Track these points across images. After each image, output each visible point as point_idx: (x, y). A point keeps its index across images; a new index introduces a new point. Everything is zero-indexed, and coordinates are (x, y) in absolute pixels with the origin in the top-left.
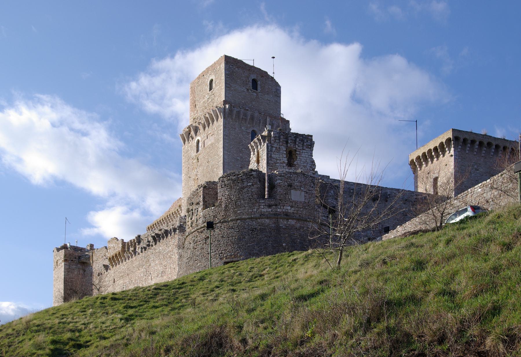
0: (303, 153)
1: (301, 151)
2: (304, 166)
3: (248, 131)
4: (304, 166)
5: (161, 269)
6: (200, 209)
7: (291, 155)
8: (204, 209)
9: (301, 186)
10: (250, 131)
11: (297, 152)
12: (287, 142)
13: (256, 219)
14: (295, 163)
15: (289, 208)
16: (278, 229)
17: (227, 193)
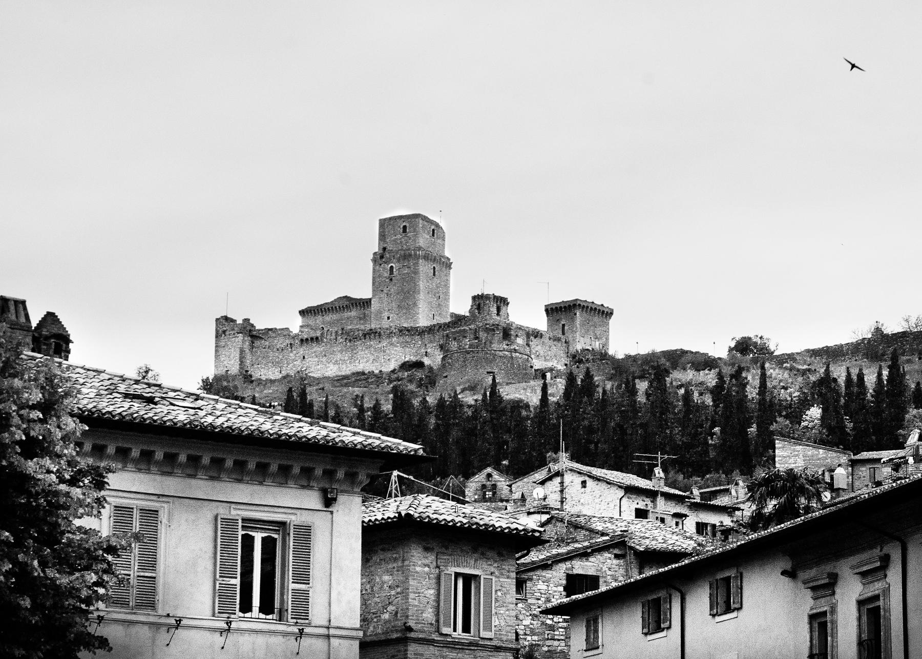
5: (372, 358)
7: (499, 309)
12: (497, 302)
16: (512, 357)
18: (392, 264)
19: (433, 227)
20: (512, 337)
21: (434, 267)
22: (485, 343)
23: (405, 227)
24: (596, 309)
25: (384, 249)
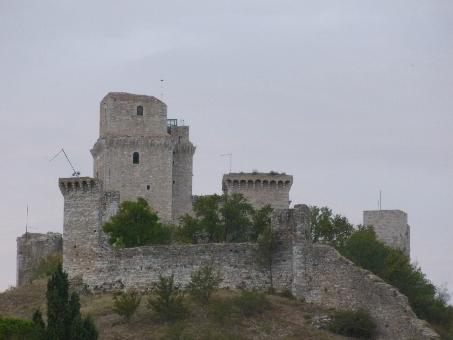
0: (111, 205)
1: (110, 204)
3: (130, 154)
10: (132, 153)
11: (106, 205)
17: (36, 250)
19: (139, 104)
24: (258, 181)
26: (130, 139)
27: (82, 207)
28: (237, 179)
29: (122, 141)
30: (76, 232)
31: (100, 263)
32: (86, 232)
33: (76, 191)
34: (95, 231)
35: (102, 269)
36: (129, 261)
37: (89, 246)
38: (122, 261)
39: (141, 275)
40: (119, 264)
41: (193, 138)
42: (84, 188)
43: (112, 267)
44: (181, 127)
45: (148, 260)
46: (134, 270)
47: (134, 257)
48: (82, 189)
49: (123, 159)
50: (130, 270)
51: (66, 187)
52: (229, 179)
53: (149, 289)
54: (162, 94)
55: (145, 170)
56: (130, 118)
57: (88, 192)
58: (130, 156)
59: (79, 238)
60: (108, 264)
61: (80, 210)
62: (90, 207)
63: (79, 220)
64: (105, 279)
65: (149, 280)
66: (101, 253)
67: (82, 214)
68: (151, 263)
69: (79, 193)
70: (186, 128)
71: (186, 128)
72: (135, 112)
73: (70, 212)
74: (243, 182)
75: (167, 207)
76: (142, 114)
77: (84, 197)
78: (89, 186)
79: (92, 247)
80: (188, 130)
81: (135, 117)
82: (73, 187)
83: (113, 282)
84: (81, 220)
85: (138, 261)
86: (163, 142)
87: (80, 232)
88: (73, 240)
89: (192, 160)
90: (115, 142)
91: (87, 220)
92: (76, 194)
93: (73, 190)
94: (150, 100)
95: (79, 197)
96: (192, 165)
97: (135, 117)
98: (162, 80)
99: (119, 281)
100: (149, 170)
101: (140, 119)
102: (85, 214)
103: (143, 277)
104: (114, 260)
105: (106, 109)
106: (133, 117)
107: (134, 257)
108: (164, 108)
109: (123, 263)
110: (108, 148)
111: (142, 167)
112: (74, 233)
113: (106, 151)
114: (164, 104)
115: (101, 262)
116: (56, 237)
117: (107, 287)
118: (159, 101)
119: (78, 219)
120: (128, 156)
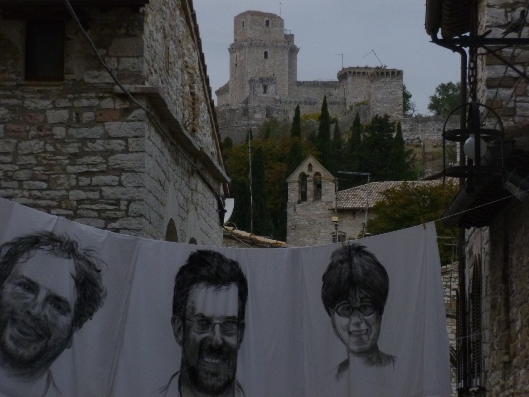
2: (271, 92)
4: (271, 92)
6: (220, 120)
7: (265, 88)
8: (221, 120)
9: (259, 112)
10: (263, 52)
13: (240, 126)
14: (267, 91)
15: (254, 121)
18: (237, 54)
19: (267, 19)
20: (250, 114)
21: (266, 53)
22: (229, 121)
23: (243, 22)
25: (236, 40)
26: (262, 42)
27: (391, 88)
28: (355, 71)
29: (258, 43)
30: (387, 105)
31: (404, 126)
32: (393, 105)
33: (386, 78)
34: (400, 105)
35: (406, 129)
36: (425, 125)
37: (396, 114)
38: (420, 125)
39: (433, 134)
40: (418, 127)
41: (297, 42)
42: (392, 77)
43: (412, 128)
44: (289, 35)
45: (438, 125)
46: (428, 131)
47: (428, 122)
48: (391, 77)
49: (258, 56)
50: (425, 131)
51: (380, 75)
52: (350, 71)
53: (439, 144)
54: (280, 13)
55: (272, 63)
56: (262, 28)
57: (394, 79)
58: (262, 53)
59: (389, 109)
60: (410, 126)
61: (390, 90)
62: (396, 88)
63: (389, 97)
64: (408, 136)
65: (439, 138)
66: (404, 120)
67: (391, 93)
68: (440, 127)
69: (388, 79)
70: (292, 36)
71: (292, 36)
72: (265, 24)
73: (382, 92)
74: (359, 73)
75: (286, 89)
76: (269, 26)
77: (392, 82)
78: (396, 75)
79: (398, 115)
80: (294, 37)
81: (264, 28)
82: (385, 75)
83: (414, 138)
84: (390, 97)
85: (431, 125)
86: (283, 45)
87: (389, 105)
88: (384, 110)
89: (296, 57)
90: (253, 44)
91: (394, 97)
92: (386, 80)
93: (384, 78)
94: (273, 16)
95: (388, 82)
96: (296, 60)
97: (264, 28)
98: (280, 3)
99: (418, 138)
100: (274, 63)
101: (267, 29)
102: (393, 93)
103: (435, 135)
104: (414, 124)
105: (243, 22)
106: (263, 27)
107: (428, 122)
108: (282, 22)
109: (420, 126)
110: (248, 48)
111: (270, 61)
112: (385, 105)
113: (247, 50)
114: (282, 19)
115: (405, 125)
116: (243, 107)
117: (409, 141)
118: (279, 17)
119: (387, 96)
120: (259, 53)
